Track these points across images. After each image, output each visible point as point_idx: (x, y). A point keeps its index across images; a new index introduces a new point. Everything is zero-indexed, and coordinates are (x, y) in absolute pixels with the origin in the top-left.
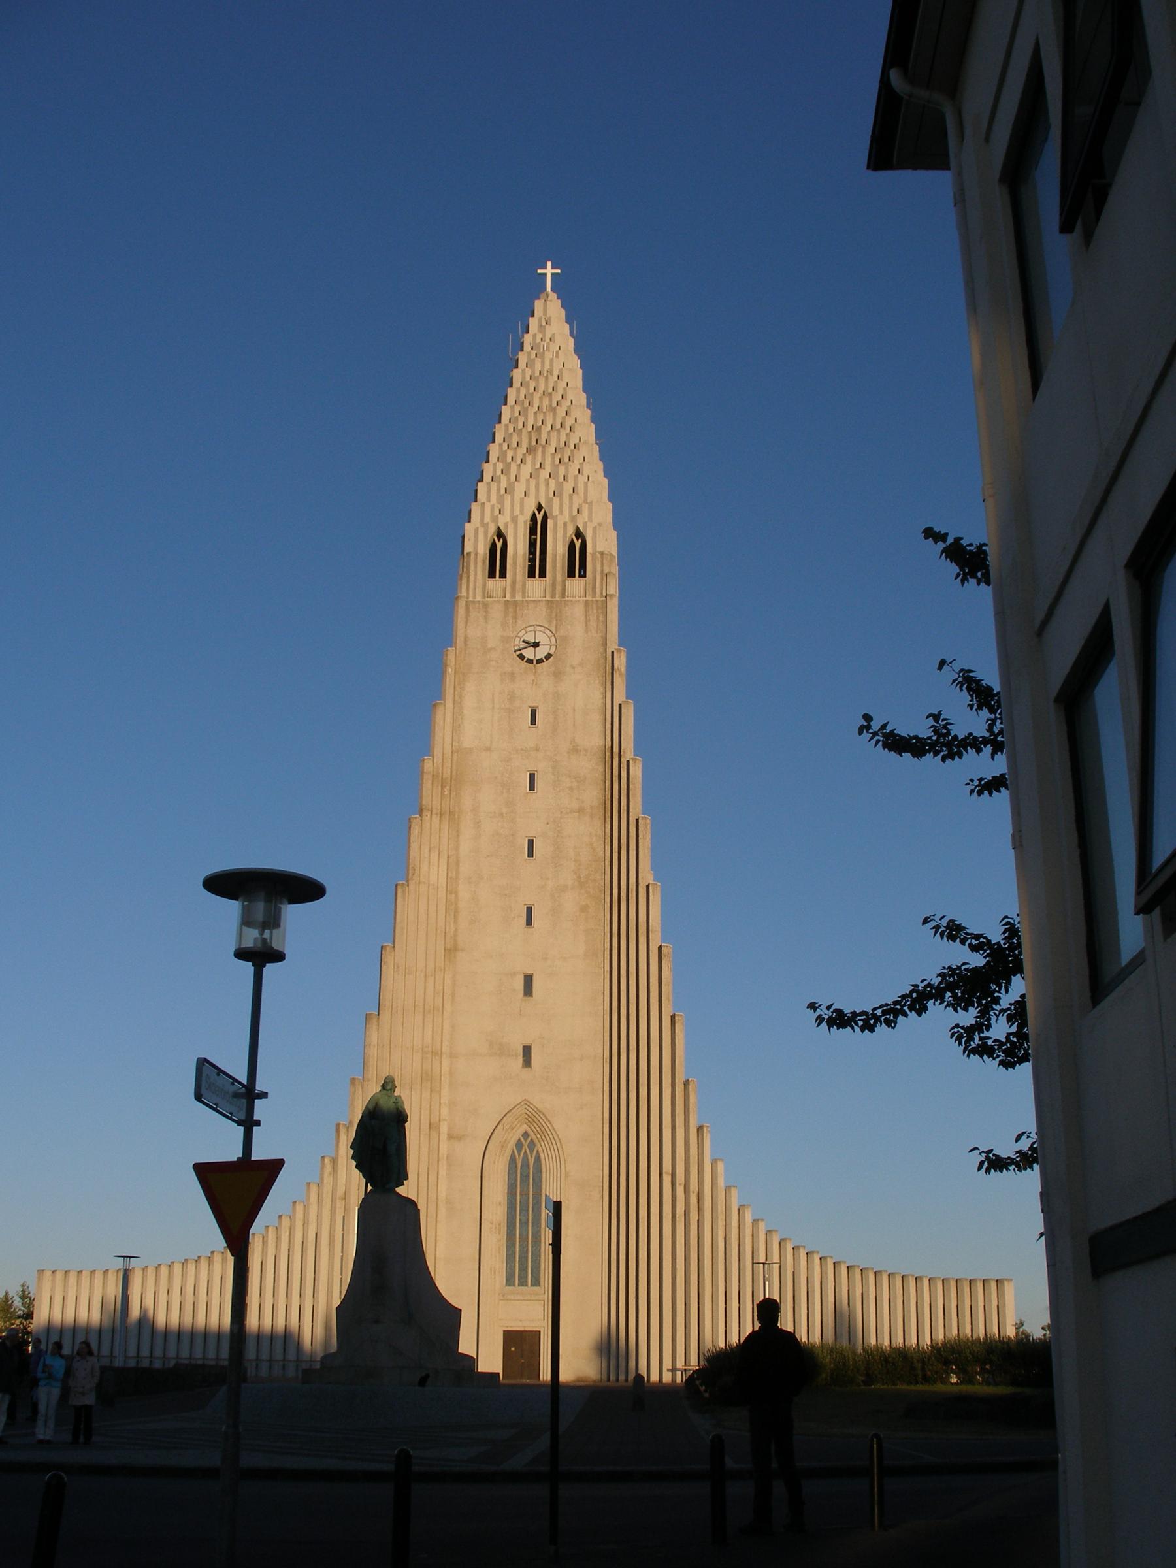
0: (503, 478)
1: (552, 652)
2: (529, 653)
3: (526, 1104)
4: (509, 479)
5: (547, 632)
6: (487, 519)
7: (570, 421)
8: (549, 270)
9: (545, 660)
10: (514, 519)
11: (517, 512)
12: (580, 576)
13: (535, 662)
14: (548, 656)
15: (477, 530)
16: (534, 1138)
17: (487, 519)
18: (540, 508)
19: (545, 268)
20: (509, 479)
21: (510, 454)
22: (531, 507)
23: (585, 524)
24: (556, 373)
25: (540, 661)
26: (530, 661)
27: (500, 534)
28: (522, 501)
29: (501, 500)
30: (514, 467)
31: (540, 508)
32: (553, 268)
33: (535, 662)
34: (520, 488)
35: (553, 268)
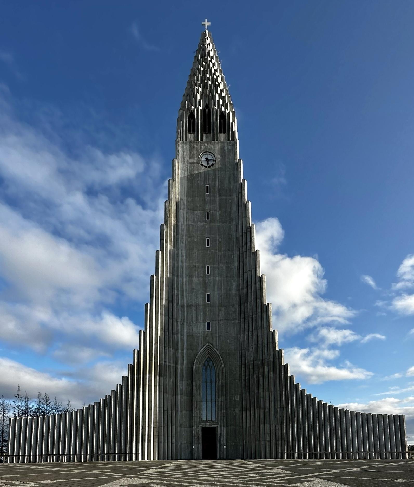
1: (214, 163)
2: (205, 164)
3: (209, 347)
5: (212, 155)
9: (211, 166)
13: (207, 167)
14: (213, 165)
16: (212, 359)
19: (205, 22)
20: (194, 93)
23: (225, 111)
25: (209, 167)
26: (205, 167)
27: (192, 115)
30: (196, 87)
31: (207, 106)
33: (207, 167)
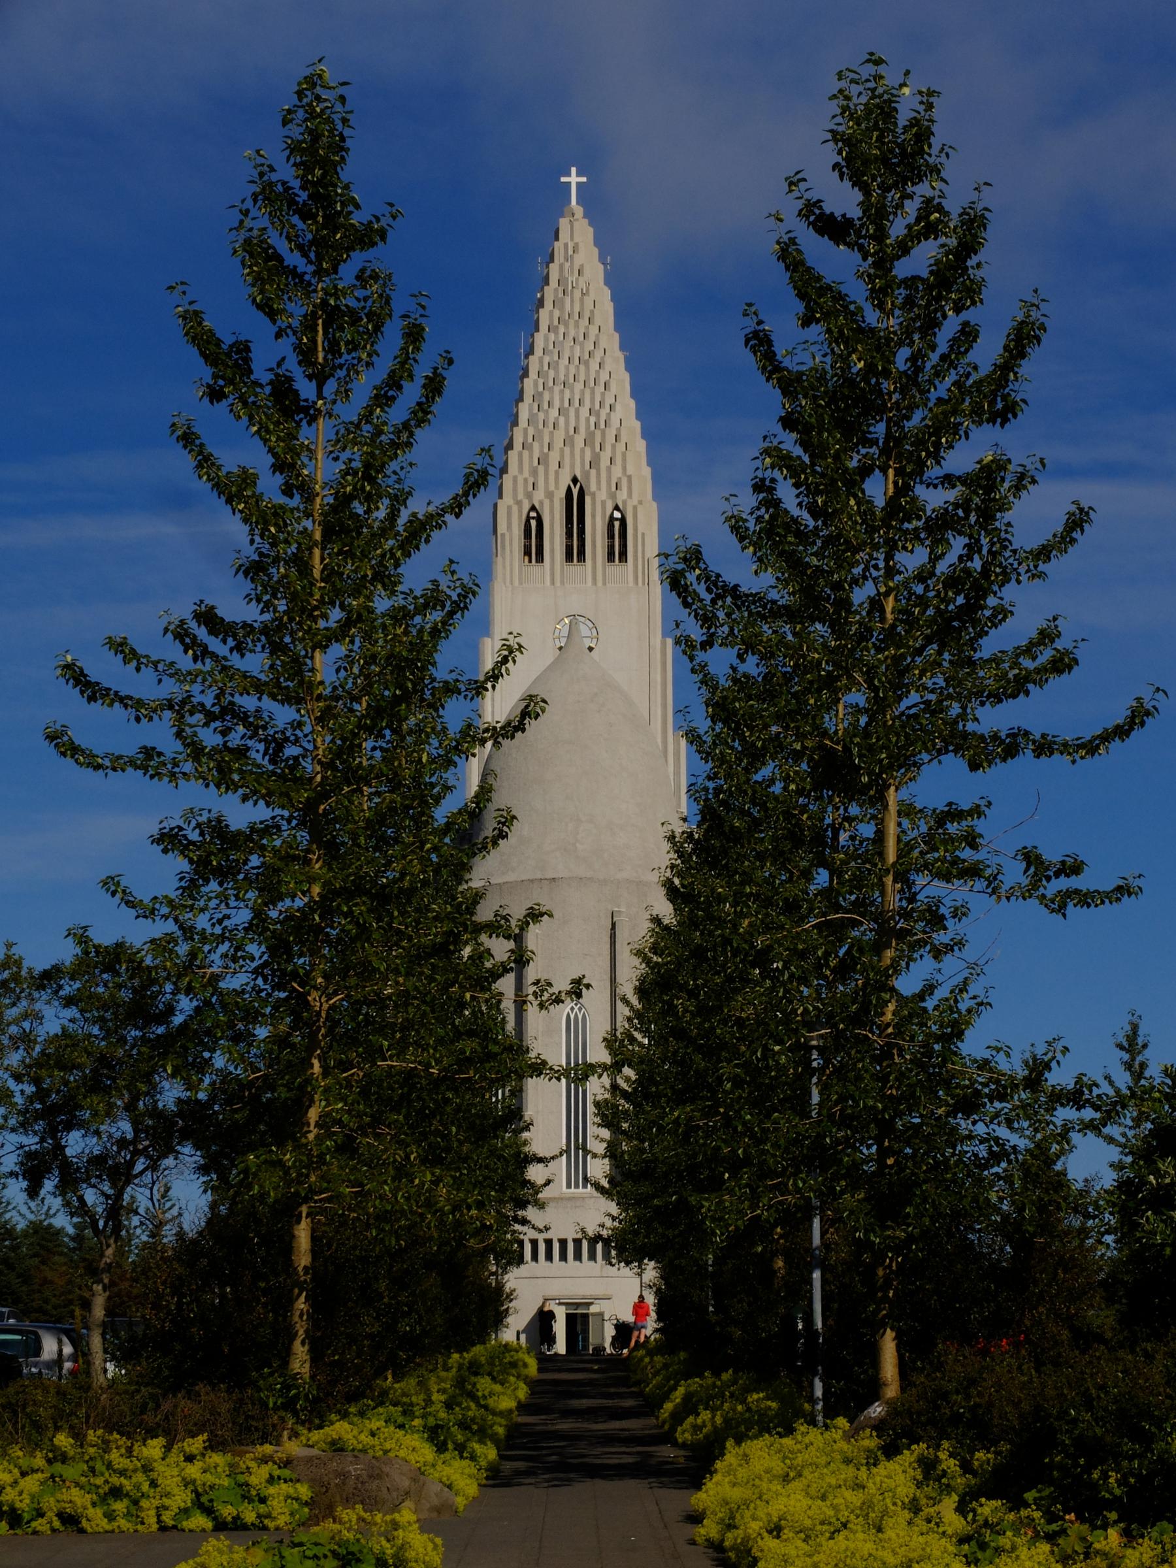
0: (536, 445)
4: (542, 446)
6: (521, 496)
7: (604, 377)
8: (574, 179)
10: (550, 495)
11: (552, 488)
12: (620, 561)
15: (509, 508)
17: (521, 496)
18: (575, 480)
20: (542, 446)
21: (541, 416)
22: (566, 481)
23: (625, 502)
24: (587, 315)
28: (557, 473)
29: (534, 472)
30: (546, 432)
31: (575, 480)
32: (578, 175)
34: (554, 457)
35: (578, 175)
